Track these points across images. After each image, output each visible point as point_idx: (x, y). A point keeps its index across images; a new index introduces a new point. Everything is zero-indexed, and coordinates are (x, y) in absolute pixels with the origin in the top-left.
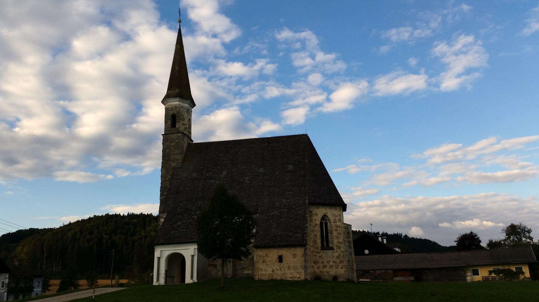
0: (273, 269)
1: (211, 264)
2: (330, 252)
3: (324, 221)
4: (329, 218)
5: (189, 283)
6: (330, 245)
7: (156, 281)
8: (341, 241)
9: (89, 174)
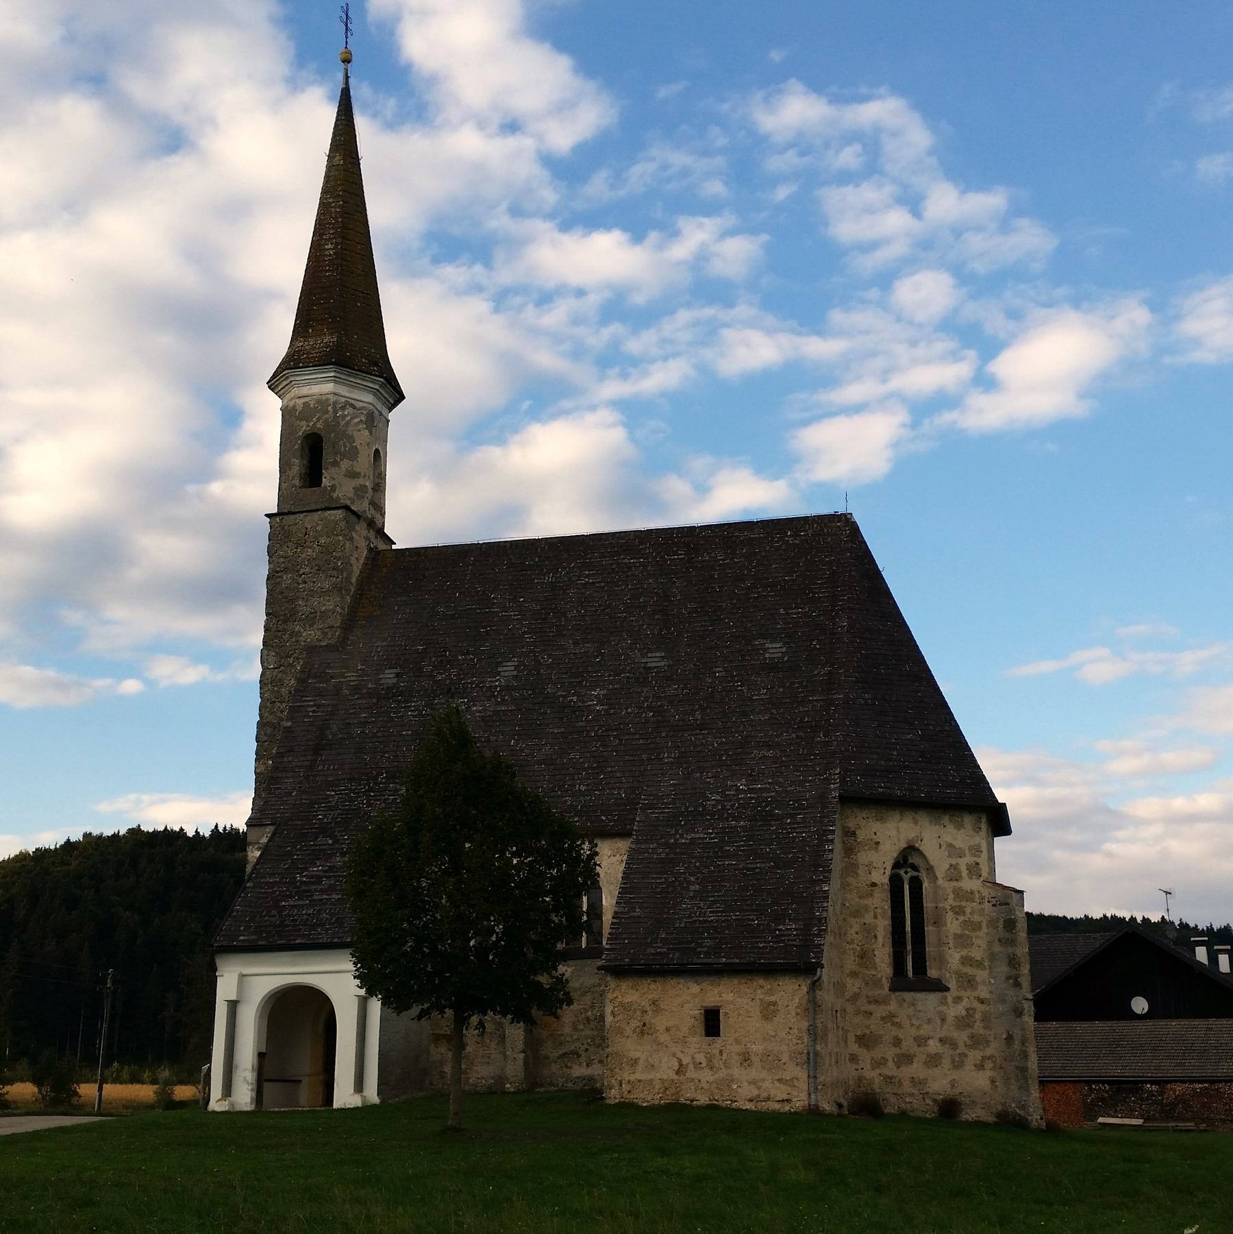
0: (680, 1061)
1: (442, 1032)
2: (929, 1001)
3: (906, 873)
4: (930, 859)
5: (348, 1106)
6: (933, 973)
8: (977, 954)
9: (51, 673)
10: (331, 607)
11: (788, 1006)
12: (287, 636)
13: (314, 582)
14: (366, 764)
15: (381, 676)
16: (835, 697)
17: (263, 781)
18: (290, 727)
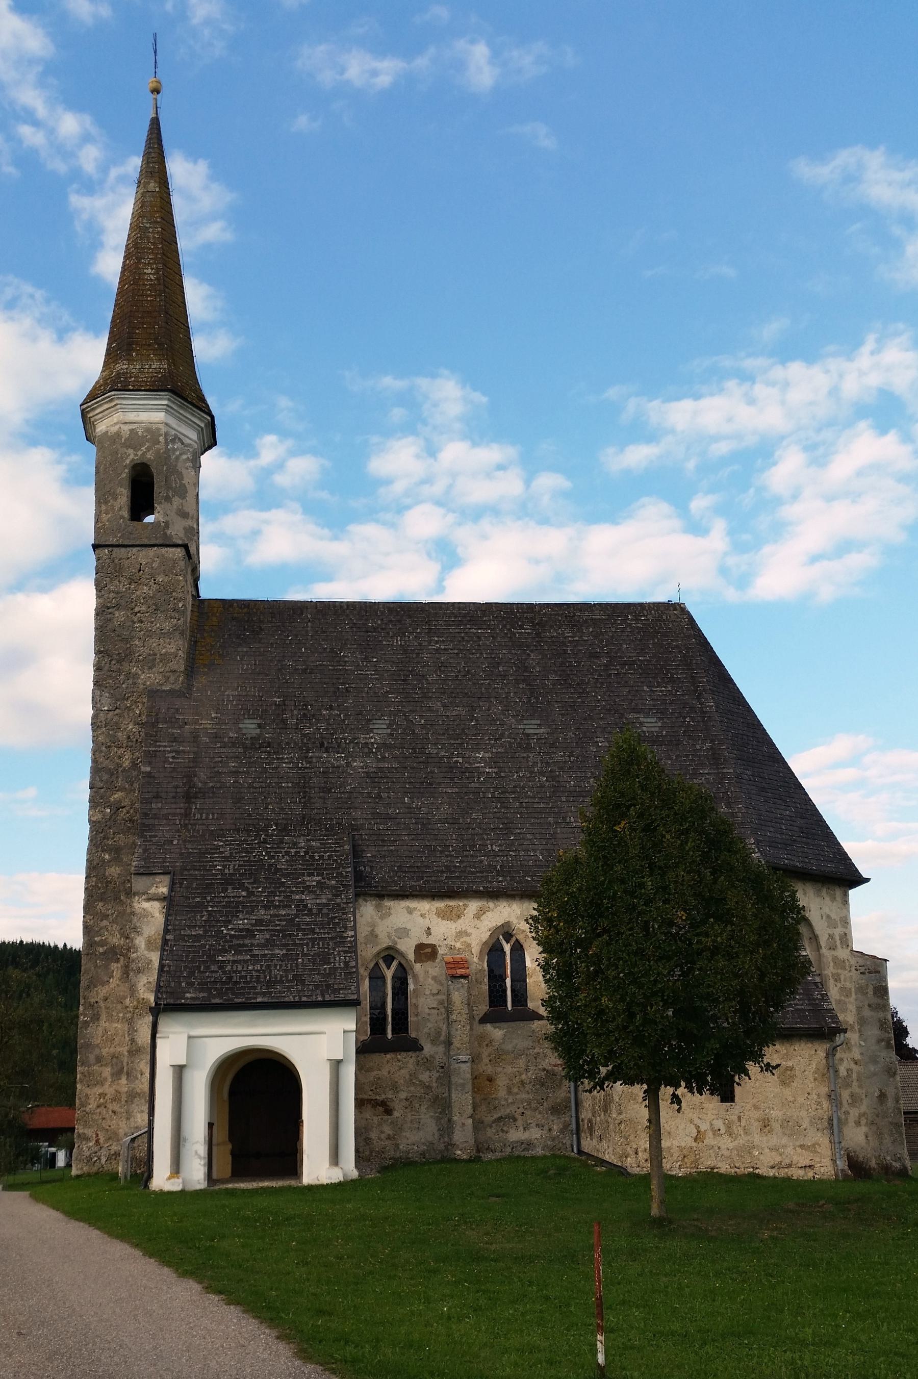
0: (697, 1127)
1: (366, 1097)
10: (172, 651)
11: (804, 1071)
12: (122, 677)
13: (152, 622)
14: (249, 815)
15: (241, 726)
16: (725, 771)
17: (100, 831)
18: (150, 772)
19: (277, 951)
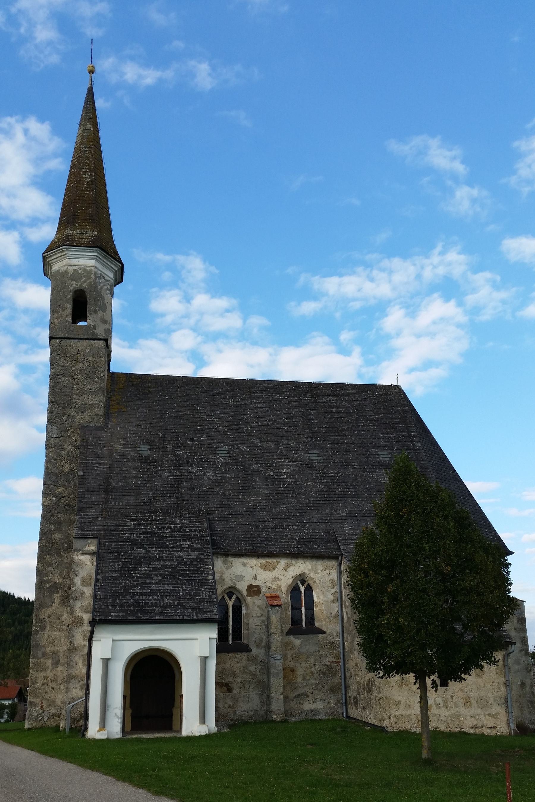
7: (98, 728)
10: (97, 402)
12: (65, 417)
14: (145, 503)
15: (138, 449)
18: (83, 476)
19: (167, 588)
